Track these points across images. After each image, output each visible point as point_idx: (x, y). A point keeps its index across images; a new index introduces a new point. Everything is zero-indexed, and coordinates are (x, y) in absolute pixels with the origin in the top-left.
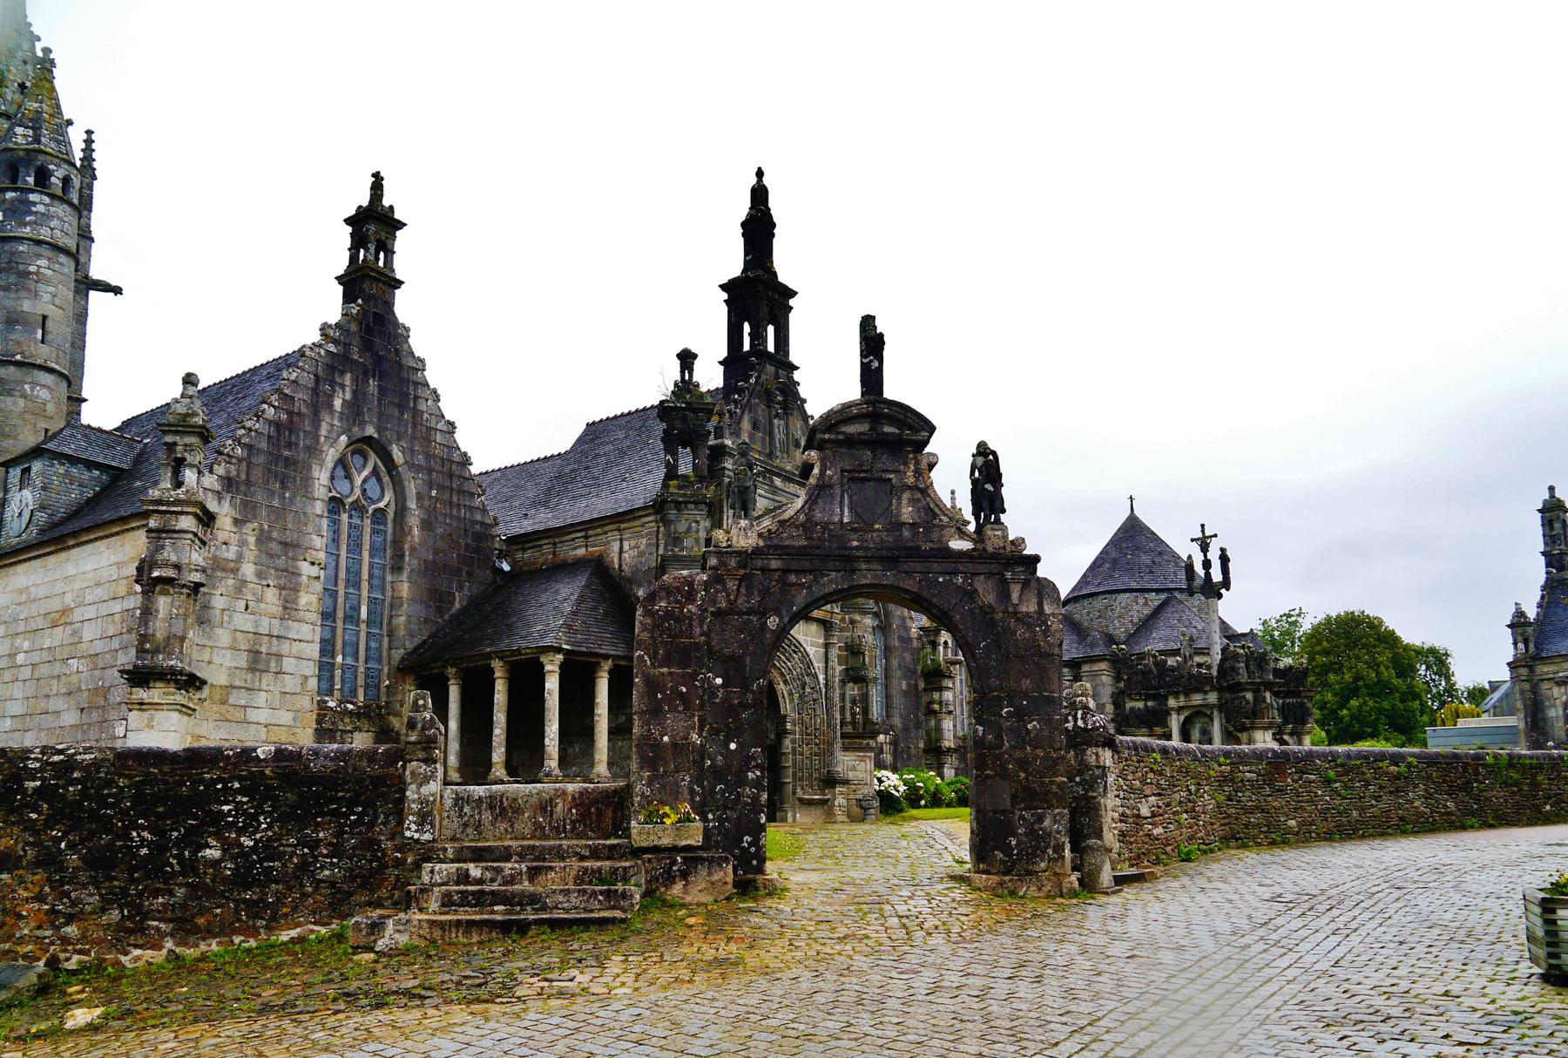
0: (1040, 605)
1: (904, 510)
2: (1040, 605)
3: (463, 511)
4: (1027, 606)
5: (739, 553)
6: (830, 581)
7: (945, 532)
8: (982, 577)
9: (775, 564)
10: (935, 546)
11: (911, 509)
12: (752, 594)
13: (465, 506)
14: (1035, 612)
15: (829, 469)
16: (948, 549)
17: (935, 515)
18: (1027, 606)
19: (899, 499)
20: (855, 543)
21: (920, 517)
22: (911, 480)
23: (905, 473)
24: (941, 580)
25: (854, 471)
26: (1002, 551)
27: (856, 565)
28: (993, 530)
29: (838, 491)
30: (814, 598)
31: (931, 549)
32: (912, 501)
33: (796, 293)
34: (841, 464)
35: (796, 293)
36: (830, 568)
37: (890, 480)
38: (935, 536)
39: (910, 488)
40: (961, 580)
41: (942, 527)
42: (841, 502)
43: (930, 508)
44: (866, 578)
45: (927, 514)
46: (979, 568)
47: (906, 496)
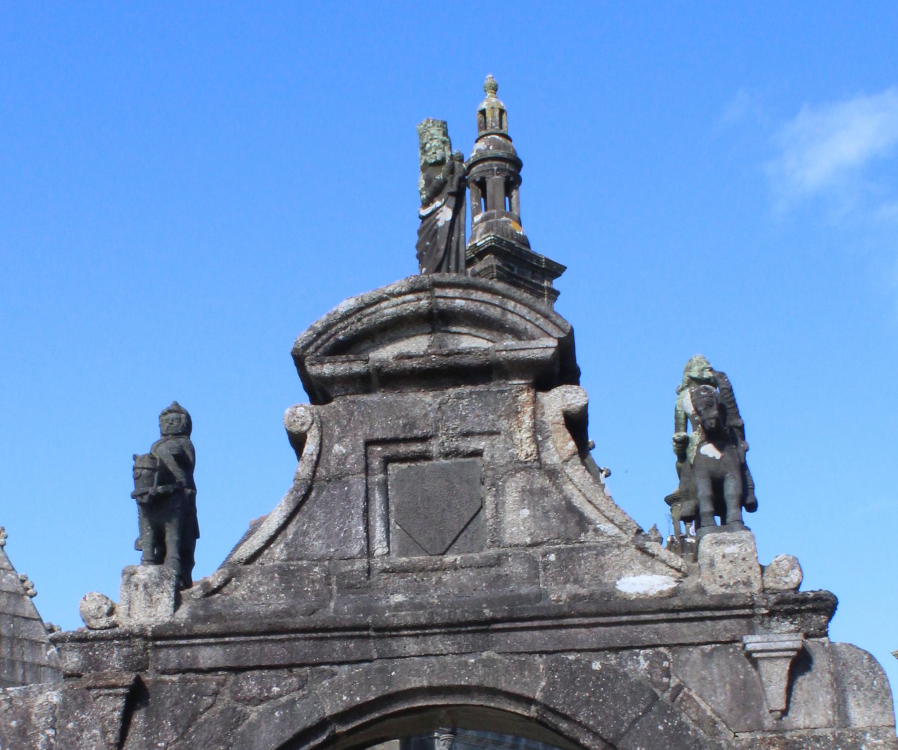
0: (840, 707)
1: (509, 517)
2: (840, 707)
3: (20, 672)
4: (809, 714)
5: (128, 637)
6: (336, 688)
7: (609, 558)
8: (696, 653)
9: (208, 656)
10: (583, 591)
11: (526, 512)
12: (160, 727)
13: (24, 663)
14: (830, 725)
15: (340, 440)
16: (611, 594)
17: (583, 522)
18: (809, 714)
19: (499, 493)
20: (398, 598)
21: (549, 530)
22: (526, 449)
23: (510, 435)
24: (596, 666)
25: (396, 441)
26: (742, 590)
27: (394, 644)
28: (719, 543)
29: (357, 484)
30: (298, 728)
31: (575, 598)
32: (531, 495)
33: (565, 268)
34: (366, 428)
35: (565, 268)
36: (336, 657)
37: (478, 453)
38: (586, 567)
39: (522, 467)
40: (644, 664)
41: (601, 551)
42: (366, 511)
43: (571, 509)
44: (418, 674)
45: (564, 521)
46: (686, 632)
47: (513, 488)
